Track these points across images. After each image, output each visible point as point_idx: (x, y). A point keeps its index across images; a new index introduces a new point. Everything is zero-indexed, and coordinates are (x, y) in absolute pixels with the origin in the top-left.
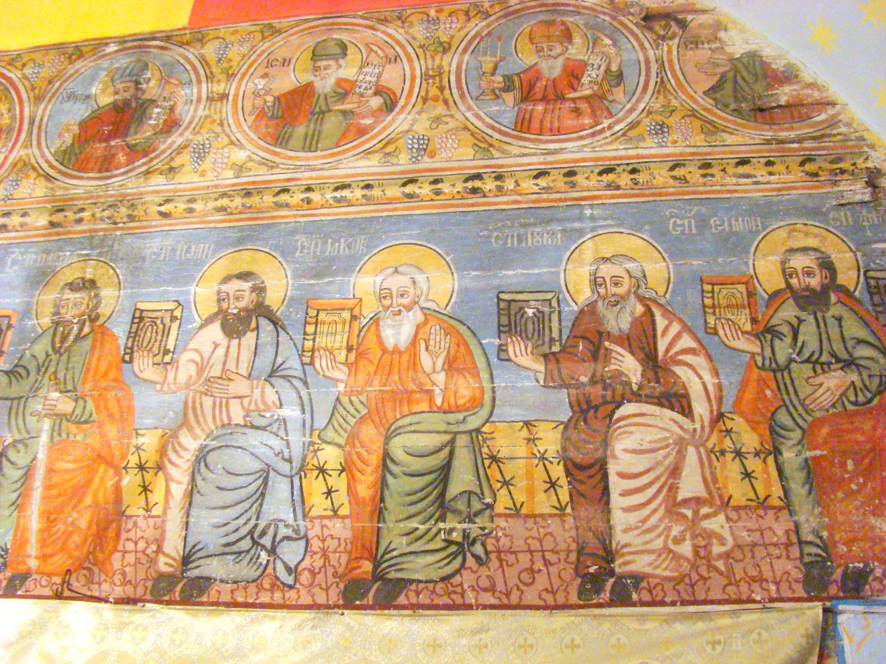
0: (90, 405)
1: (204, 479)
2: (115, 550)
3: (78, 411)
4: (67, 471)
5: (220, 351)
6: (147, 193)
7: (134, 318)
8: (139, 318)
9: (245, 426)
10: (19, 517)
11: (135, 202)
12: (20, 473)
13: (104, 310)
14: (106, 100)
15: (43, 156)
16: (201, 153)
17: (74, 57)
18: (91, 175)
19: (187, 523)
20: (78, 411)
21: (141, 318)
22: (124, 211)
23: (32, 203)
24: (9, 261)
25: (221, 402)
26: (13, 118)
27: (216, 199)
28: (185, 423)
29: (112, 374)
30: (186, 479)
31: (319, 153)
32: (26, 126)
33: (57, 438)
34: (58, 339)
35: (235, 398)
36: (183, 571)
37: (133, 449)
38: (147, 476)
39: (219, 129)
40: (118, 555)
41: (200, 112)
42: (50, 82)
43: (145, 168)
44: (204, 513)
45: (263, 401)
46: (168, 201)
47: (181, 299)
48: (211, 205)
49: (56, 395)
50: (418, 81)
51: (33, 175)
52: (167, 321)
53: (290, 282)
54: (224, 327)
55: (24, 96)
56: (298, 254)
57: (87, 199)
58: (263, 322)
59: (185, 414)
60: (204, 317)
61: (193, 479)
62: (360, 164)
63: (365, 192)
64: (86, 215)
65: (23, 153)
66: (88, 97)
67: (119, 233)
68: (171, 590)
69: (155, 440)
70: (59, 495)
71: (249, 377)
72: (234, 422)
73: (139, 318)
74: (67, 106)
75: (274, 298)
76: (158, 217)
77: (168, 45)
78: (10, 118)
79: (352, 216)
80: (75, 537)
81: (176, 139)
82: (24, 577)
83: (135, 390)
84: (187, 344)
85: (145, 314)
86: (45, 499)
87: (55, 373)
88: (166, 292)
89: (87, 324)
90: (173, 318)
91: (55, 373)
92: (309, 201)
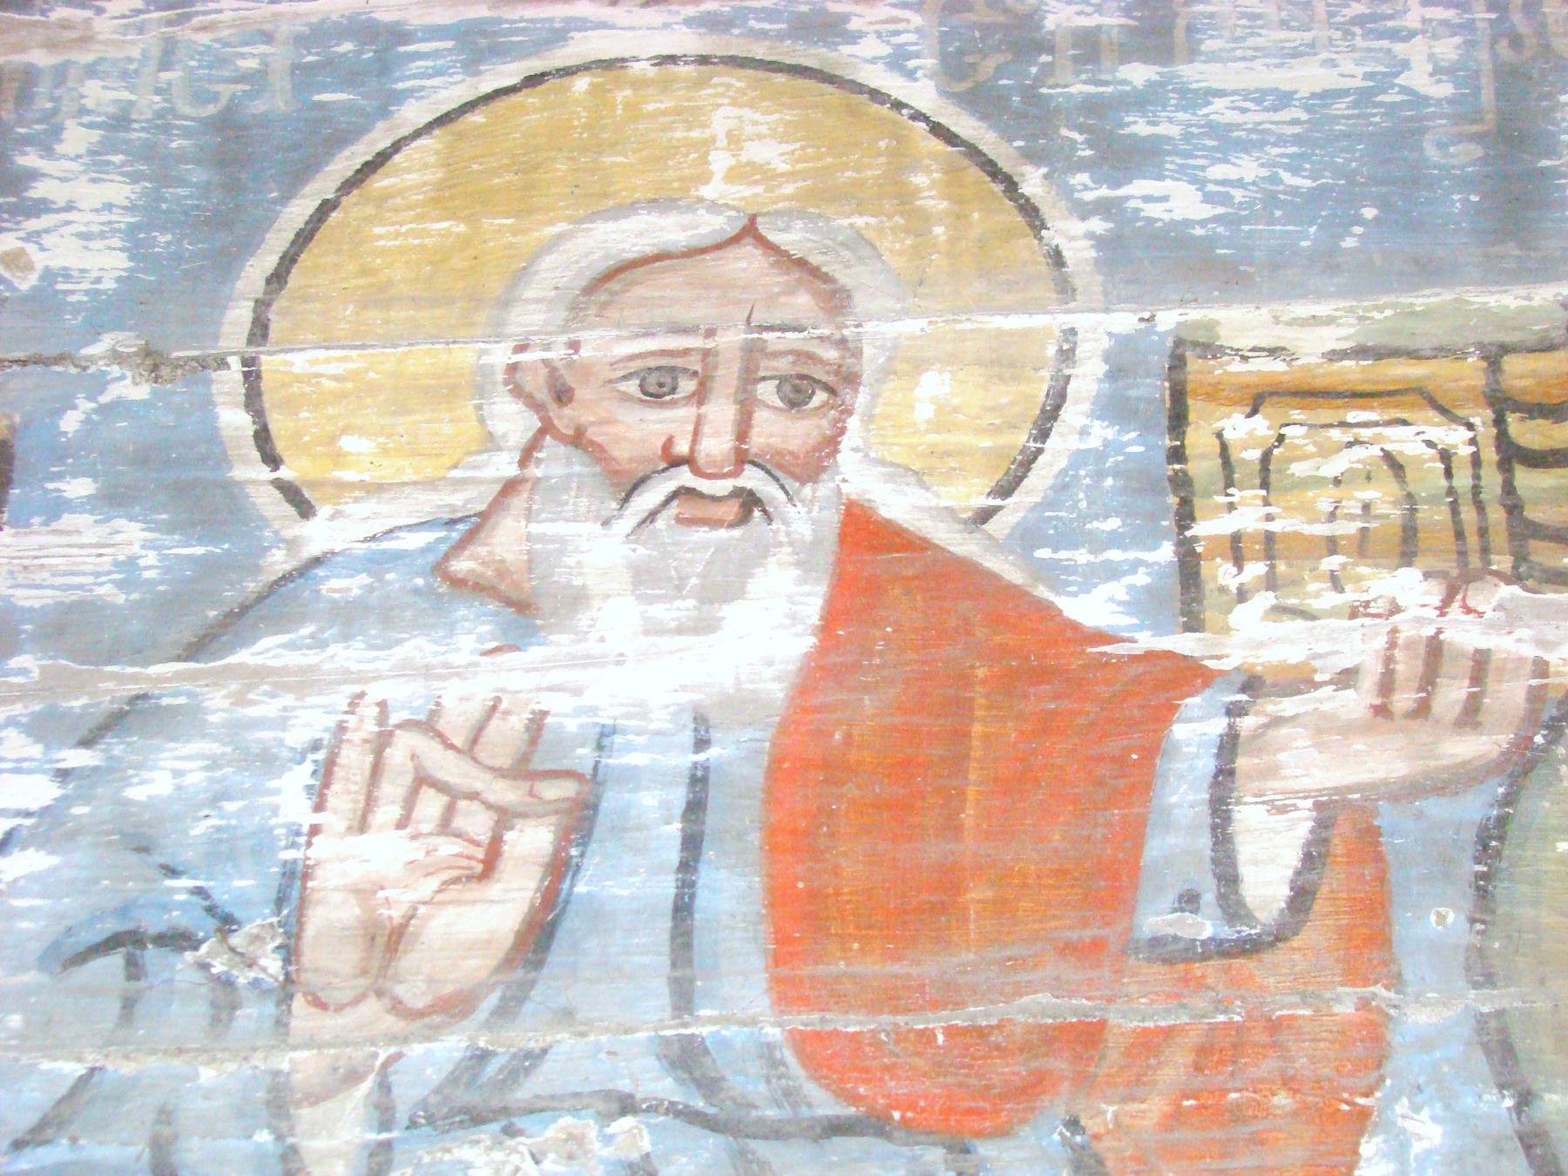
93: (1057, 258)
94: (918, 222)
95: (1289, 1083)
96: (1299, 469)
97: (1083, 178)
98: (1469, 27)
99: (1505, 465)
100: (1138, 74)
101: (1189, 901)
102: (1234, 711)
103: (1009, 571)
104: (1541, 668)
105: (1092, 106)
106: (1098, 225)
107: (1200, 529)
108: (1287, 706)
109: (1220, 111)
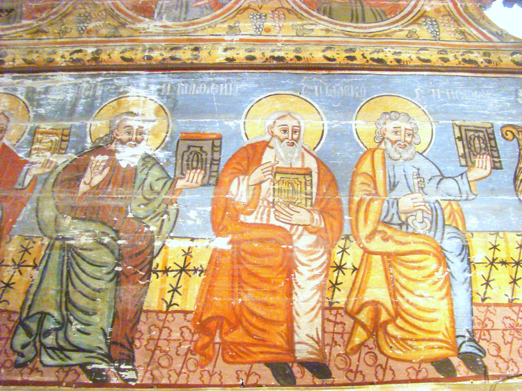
93: (29, 117)
94: (18, 112)
95: (20, 202)
96: (43, 141)
97: (34, 108)
98: (74, 93)
99: (61, 142)
100: (43, 96)
101: (20, 185)
102: (30, 166)
103: (15, 151)
104: (56, 163)
105: (39, 100)
106: (34, 113)
107: (34, 147)
108: (34, 166)
109: (49, 101)
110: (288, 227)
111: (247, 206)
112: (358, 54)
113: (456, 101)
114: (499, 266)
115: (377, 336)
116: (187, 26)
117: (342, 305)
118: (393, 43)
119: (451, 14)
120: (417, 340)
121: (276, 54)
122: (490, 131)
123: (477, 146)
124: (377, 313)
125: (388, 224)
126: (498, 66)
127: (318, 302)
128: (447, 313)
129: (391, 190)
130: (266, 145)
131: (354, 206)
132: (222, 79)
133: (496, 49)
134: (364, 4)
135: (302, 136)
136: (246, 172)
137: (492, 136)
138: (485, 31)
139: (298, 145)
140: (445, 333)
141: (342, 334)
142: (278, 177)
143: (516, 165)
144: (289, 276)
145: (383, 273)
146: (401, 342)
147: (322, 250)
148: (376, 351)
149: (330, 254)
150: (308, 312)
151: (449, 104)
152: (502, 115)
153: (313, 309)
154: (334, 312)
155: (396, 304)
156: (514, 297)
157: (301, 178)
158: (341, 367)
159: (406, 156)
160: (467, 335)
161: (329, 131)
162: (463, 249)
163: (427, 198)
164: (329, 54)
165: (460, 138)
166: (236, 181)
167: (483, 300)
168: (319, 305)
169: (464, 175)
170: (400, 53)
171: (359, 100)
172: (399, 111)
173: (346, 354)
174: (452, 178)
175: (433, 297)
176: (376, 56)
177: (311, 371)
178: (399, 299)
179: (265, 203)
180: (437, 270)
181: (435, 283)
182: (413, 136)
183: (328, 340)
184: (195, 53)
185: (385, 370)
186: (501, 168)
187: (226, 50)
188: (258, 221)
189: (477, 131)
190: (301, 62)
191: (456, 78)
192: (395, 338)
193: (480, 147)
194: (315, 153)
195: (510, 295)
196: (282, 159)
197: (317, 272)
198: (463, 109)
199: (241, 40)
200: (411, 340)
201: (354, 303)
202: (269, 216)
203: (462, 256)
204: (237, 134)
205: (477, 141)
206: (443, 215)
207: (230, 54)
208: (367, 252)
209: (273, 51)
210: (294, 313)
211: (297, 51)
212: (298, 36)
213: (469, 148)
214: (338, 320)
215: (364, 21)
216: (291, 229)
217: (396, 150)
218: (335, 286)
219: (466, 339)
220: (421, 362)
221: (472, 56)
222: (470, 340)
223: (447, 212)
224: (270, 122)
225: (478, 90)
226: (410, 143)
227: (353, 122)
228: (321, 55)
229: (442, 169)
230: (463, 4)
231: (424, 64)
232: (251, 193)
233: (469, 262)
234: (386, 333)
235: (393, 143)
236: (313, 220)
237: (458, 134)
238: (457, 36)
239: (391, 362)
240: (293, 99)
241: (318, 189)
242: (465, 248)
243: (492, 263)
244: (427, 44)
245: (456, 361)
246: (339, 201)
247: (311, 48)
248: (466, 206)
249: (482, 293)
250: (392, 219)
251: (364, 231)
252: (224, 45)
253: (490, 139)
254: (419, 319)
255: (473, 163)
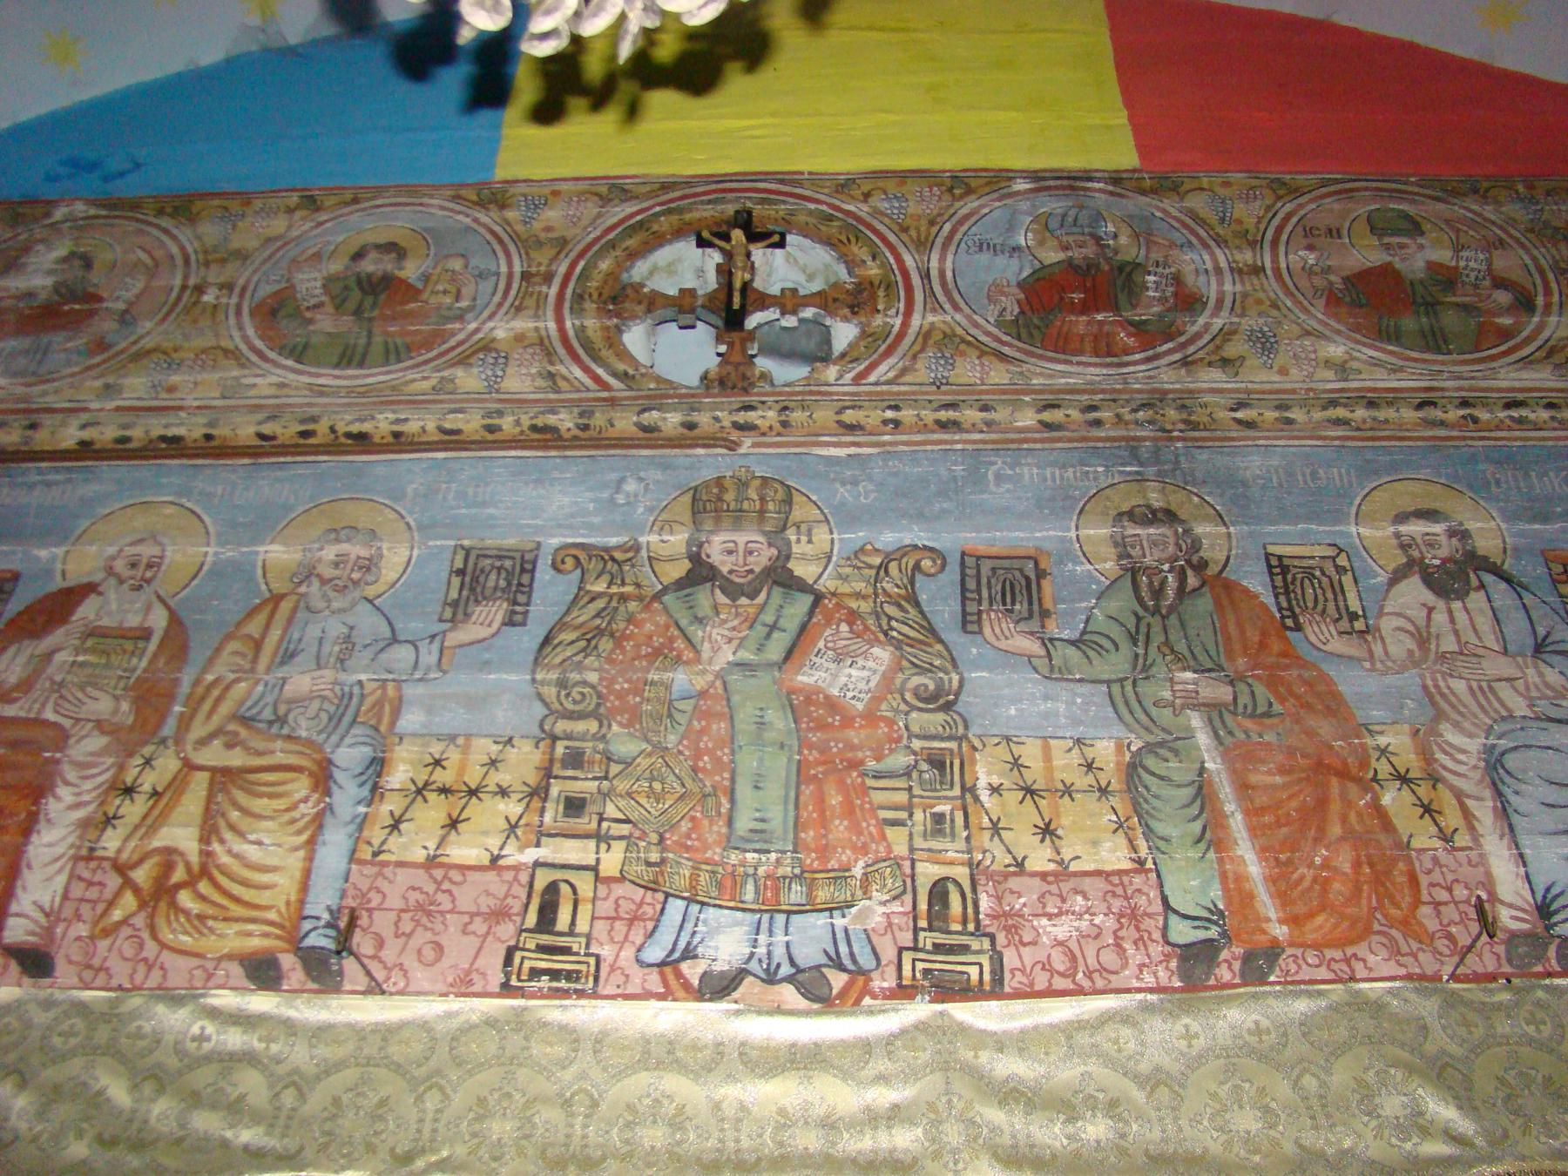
0: (1261, 690)
1: (1517, 793)
2: (1417, 902)
3: (1244, 699)
4: (1274, 787)
5: (1440, 617)
6: (1200, 391)
7: (1270, 567)
8: (1278, 568)
9: (1538, 718)
10: (1221, 861)
11: (1187, 402)
12: (1189, 792)
13: (1213, 552)
14: (1052, 256)
15: (976, 325)
16: (1266, 344)
17: (957, 192)
18: (1084, 359)
19: (1521, 856)
20: (1244, 699)
21: (1285, 570)
22: (1172, 414)
23: (987, 392)
24: (991, 477)
25: (1481, 688)
26: (885, 265)
27: (1324, 408)
28: (1439, 716)
29: (1276, 646)
30: (1488, 793)
31: (1455, 356)
32: (916, 281)
33: (1228, 740)
34: (1145, 593)
35: (1500, 680)
36: (1548, 928)
37: (1375, 754)
38: (1421, 791)
39: (1275, 313)
40: (1425, 910)
41: (1228, 287)
42: (932, 223)
43: (1177, 356)
44: (1541, 841)
45: (1547, 685)
46: (1241, 405)
47: (1340, 542)
48: (1318, 415)
49: (1189, 675)
50: (1551, 276)
51: (974, 354)
52: (1331, 571)
53: (1503, 526)
54: (1428, 581)
55: (892, 238)
56: (1494, 489)
57: (1094, 392)
58: (1488, 578)
59: (1433, 703)
60: (1390, 568)
61: (1499, 794)
62: (1524, 375)
63: (1553, 413)
64: (1105, 415)
65: (931, 318)
66: (1016, 249)
67: (1179, 445)
68: (1541, 957)
69: (1406, 740)
70: (1278, 824)
71: (1505, 652)
72: (1518, 713)
73: (1278, 568)
74: (984, 258)
75: (1487, 544)
76: (1236, 426)
77: (1119, 190)
78: (882, 266)
79: (1550, 443)
80: (1336, 886)
81: (1210, 321)
82: (1273, 952)
83: (1331, 670)
84: (1382, 607)
85: (1286, 562)
86: (1253, 831)
87: (1167, 643)
88: (1307, 531)
89: (1189, 572)
90: (1341, 570)
91: (1167, 643)
92: (1475, 420)
110: (67, 723)
111: (17, 687)
112: (322, 427)
113: (484, 504)
114: (432, 796)
115: (155, 908)
116: (30, 385)
117: (111, 853)
118: (399, 402)
119: (546, 342)
120: (225, 919)
121: (170, 432)
122: (528, 557)
123: (491, 583)
124: (168, 867)
125: (246, 721)
126: (603, 435)
127: (72, 846)
128: (298, 875)
129: (282, 663)
130: (90, 589)
131: (200, 690)
132: (58, 477)
133: (612, 402)
134: (376, 331)
135: (160, 575)
136: (36, 633)
137: (528, 567)
138: (600, 371)
139: (148, 589)
140: (283, 910)
141: (94, 902)
142: (89, 643)
143: (557, 618)
144: (36, 802)
145: (202, 803)
146: (196, 922)
147: (110, 761)
148: (146, 935)
149: (122, 768)
150: (46, 865)
151: (464, 511)
152: (571, 527)
153: (57, 859)
154: (93, 864)
155: (207, 855)
156: (440, 852)
157: (129, 645)
158: (75, 958)
159: (335, 605)
160: (326, 916)
161: (215, 563)
162: (371, 763)
163: (342, 677)
164: (267, 429)
165: (461, 572)
166: (11, 651)
167: (376, 854)
168: (72, 852)
169: (438, 638)
170: (406, 420)
171: (291, 508)
172: (360, 526)
173: (92, 937)
174: (413, 643)
175: (279, 845)
176: (356, 428)
177: (21, 963)
178: (216, 847)
179: (47, 685)
180: (305, 800)
181: (293, 821)
182: (368, 569)
183: (68, 911)
184: (30, 433)
185: (150, 968)
186: (523, 624)
187: (84, 427)
188: (22, 714)
189: (500, 558)
190: (213, 443)
191: (501, 462)
192: (186, 913)
193: (496, 588)
194: (172, 603)
195: (432, 845)
196: (109, 614)
197: (86, 798)
198: (492, 517)
199: (118, 409)
200: (215, 918)
201: (133, 851)
202: (43, 705)
203: (364, 778)
204: (49, 573)
205: (493, 576)
206: (360, 704)
207: (86, 435)
208: (189, 766)
209: (166, 426)
210: (24, 864)
211: (211, 424)
212: (224, 397)
213: (472, 589)
214: (96, 879)
215: (361, 365)
216: (73, 726)
217: (325, 595)
218: (109, 821)
219: (322, 923)
220: (220, 959)
221: (551, 420)
222: (329, 925)
223: (369, 701)
224: (111, 550)
225: (539, 482)
226: (356, 583)
227: (261, 549)
228: (252, 430)
229: (399, 626)
230: (577, 322)
231: (447, 438)
232: (31, 668)
233: (375, 787)
234: (173, 904)
235: (324, 582)
236: (116, 711)
237: (459, 564)
238: (540, 382)
239: (167, 956)
240: (170, 510)
241: (151, 662)
242: (378, 765)
243: (419, 792)
244: (467, 401)
245: (288, 961)
246: (176, 682)
247: (238, 418)
248: (410, 691)
249: (376, 842)
250: (259, 713)
251: (198, 730)
252: (84, 417)
253: (523, 570)
254: (245, 883)
255: (467, 615)
